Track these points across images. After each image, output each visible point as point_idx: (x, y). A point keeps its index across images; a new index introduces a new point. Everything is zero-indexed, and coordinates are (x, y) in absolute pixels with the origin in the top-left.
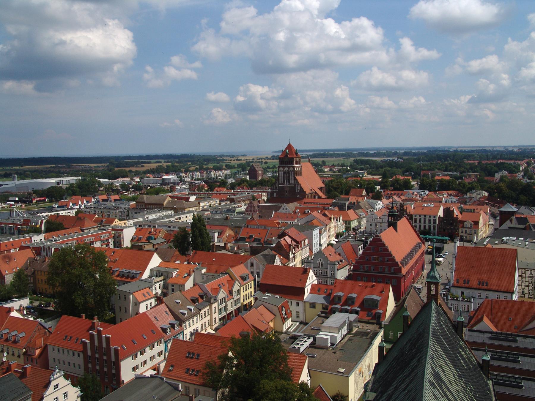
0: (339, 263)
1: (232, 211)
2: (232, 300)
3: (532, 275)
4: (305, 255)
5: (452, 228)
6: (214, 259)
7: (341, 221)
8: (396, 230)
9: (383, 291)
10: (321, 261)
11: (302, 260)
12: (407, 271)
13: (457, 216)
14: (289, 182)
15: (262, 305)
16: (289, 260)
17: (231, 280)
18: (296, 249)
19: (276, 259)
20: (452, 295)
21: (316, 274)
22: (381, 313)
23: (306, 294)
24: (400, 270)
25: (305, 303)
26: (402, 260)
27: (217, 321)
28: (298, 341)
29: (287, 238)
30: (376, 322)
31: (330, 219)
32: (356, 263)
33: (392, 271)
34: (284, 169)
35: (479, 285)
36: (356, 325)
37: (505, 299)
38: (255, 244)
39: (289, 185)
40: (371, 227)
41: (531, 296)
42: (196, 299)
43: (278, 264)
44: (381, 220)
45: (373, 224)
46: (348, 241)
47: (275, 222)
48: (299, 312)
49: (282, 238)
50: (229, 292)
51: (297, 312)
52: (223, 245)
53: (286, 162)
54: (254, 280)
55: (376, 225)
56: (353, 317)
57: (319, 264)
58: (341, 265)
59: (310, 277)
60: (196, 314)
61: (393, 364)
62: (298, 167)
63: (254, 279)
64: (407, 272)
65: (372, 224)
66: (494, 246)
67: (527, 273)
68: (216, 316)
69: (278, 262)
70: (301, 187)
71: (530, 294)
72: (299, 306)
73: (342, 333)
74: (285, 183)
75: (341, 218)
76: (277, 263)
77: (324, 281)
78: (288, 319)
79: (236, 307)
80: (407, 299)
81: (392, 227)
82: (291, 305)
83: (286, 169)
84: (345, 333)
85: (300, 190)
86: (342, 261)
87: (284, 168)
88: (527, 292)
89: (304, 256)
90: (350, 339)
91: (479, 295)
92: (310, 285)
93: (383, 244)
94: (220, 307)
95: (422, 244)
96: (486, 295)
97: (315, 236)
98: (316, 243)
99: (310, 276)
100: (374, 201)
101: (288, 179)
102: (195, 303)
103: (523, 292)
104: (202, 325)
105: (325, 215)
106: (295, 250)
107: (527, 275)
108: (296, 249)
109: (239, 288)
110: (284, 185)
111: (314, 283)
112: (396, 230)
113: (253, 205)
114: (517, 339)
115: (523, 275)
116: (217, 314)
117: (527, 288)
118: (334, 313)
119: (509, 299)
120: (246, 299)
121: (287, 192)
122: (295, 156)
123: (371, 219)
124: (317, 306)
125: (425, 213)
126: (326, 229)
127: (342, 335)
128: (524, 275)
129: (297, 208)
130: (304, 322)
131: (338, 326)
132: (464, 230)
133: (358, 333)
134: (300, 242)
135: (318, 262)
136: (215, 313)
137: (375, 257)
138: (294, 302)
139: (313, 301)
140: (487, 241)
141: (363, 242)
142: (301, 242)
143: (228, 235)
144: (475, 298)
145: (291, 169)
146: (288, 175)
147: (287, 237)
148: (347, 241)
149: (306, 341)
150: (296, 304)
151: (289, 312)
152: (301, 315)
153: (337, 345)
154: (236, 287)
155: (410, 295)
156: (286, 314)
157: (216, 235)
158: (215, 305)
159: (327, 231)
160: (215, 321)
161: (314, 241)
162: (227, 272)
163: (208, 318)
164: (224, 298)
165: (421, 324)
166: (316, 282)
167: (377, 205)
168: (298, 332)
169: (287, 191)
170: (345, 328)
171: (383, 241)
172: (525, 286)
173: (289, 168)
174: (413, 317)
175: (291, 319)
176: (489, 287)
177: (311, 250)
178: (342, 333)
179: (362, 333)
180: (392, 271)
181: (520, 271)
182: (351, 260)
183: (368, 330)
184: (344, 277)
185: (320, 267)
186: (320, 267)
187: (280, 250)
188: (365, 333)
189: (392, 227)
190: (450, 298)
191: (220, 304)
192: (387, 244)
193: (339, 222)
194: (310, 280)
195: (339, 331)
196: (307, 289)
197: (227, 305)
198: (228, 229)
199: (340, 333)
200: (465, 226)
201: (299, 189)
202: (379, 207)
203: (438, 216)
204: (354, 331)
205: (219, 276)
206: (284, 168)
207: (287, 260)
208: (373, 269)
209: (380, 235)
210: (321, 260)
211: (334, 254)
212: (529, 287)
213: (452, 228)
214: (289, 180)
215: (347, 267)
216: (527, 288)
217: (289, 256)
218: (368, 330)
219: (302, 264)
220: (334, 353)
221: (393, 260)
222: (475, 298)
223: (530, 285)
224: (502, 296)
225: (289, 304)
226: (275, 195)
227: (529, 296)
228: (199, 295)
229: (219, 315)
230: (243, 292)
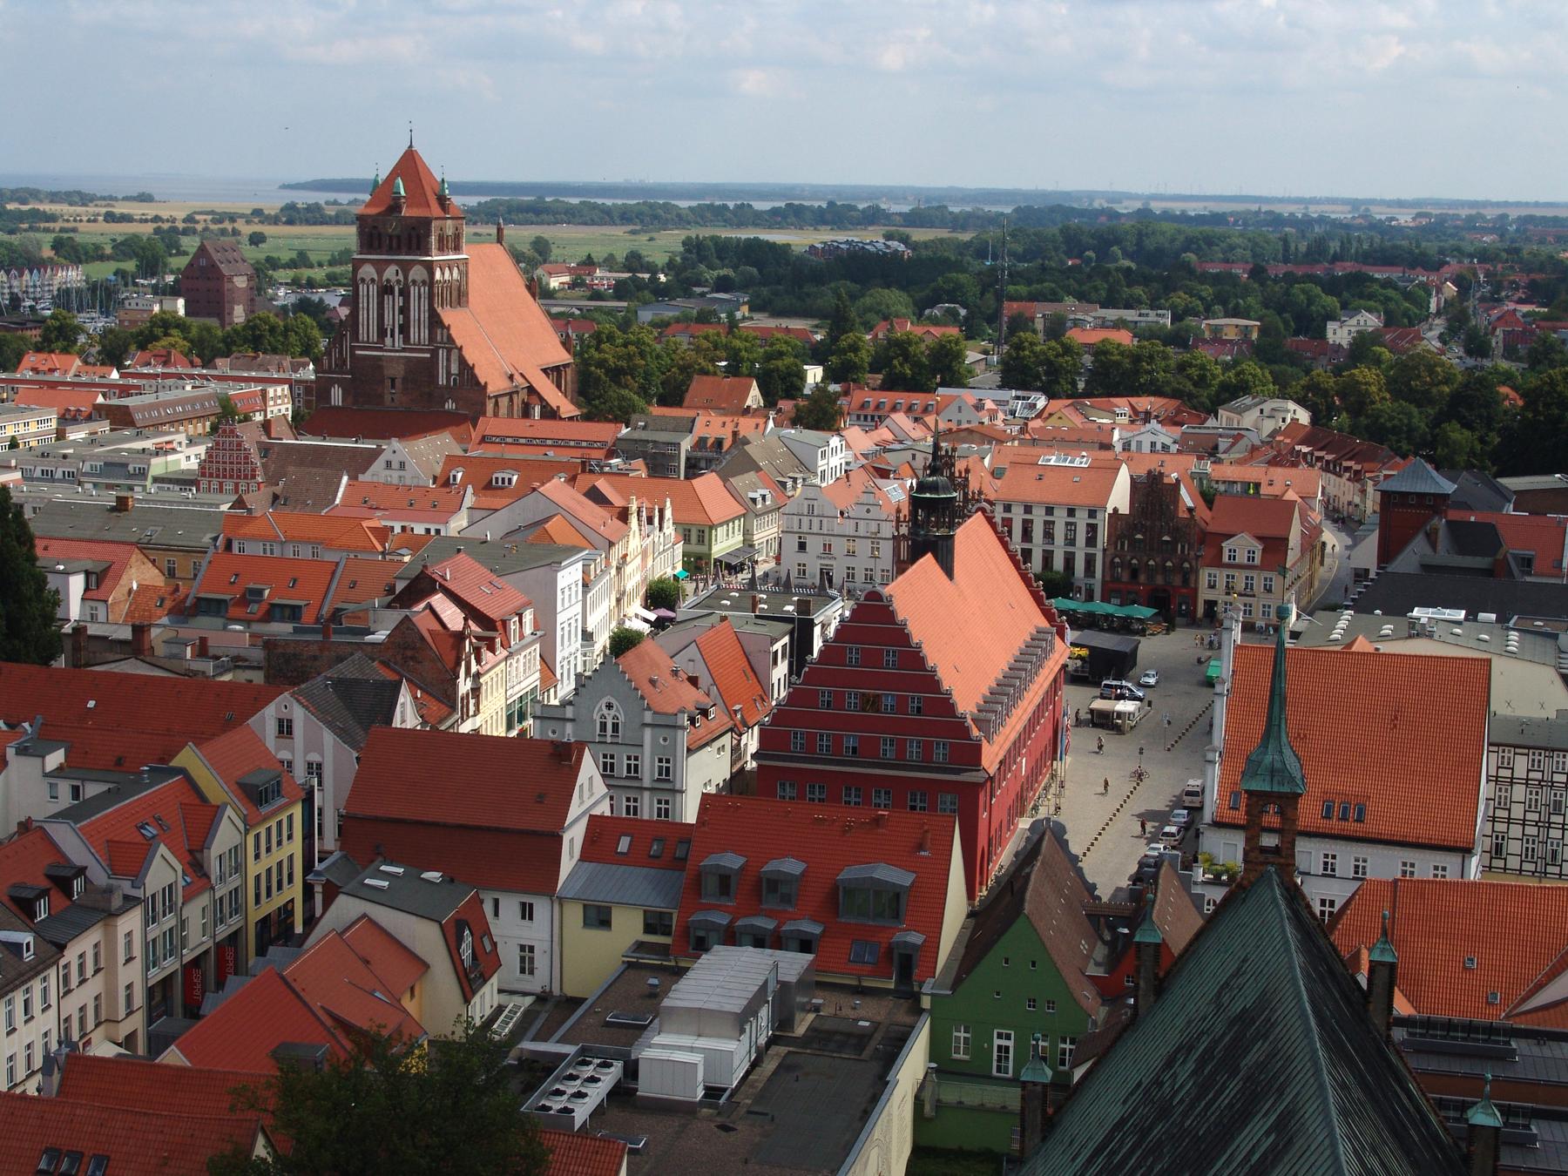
0: (692, 720)
1: (131, 468)
2: (204, 900)
3: (1539, 776)
4: (523, 685)
5: (1169, 564)
6: (91, 704)
7: (669, 528)
8: (949, 573)
9: (920, 847)
10: (613, 712)
11: (508, 707)
12: (1001, 757)
13: (1190, 510)
14: (407, 339)
15: (365, 916)
16: (453, 708)
17: (197, 801)
18: (487, 655)
19: (401, 700)
20: (1211, 861)
21: (608, 771)
22: (914, 946)
23: (568, 862)
24: (977, 749)
25: (561, 906)
26: (978, 705)
27: (139, 999)
28: (557, 1080)
29: (439, 601)
30: (892, 986)
31: (624, 515)
32: (775, 721)
33: (939, 755)
34: (380, 273)
35: (1328, 817)
36: (805, 1000)
37: (1435, 876)
38: (282, 629)
39: (404, 350)
40: (802, 558)
41: (1531, 867)
42: (38, 897)
43: (409, 725)
44: (853, 522)
45: (815, 545)
46: (724, 619)
47: (365, 524)
48: (532, 949)
49: (417, 601)
50: (189, 858)
51: (522, 948)
52: (126, 633)
53: (391, 237)
54: (304, 801)
55: (827, 548)
56: (793, 964)
57: (603, 726)
58: (702, 731)
59: (582, 786)
60: (38, 969)
61: (1113, 1153)
62: (450, 265)
63: (303, 795)
64: (1001, 762)
65: (809, 540)
66: (1385, 648)
67: (1521, 765)
68: (131, 975)
69: (406, 714)
70: (462, 362)
71: (1527, 855)
72: (531, 918)
73: (754, 1039)
74: (388, 340)
75: (668, 513)
76: (403, 721)
77: (625, 803)
78: (485, 981)
79: (223, 932)
80: (1033, 877)
81: (929, 555)
82: (496, 914)
83: (390, 273)
84: (762, 1040)
85: (460, 373)
86: (704, 713)
87: (380, 266)
88: (1514, 847)
89: (517, 689)
90: (784, 1067)
91: (1326, 863)
92: (584, 822)
93: (900, 635)
94: (155, 931)
95: (1057, 637)
96: (1357, 860)
97: (566, 590)
98: (567, 629)
99: (582, 778)
100: (811, 436)
101: (399, 319)
102: (32, 915)
103: (1499, 848)
104: (67, 1020)
105: (595, 496)
106: (479, 661)
107: (1520, 772)
109: (237, 839)
110: (380, 349)
111: (597, 811)
112: (949, 573)
113: (239, 444)
114: (1514, 1045)
115: (1503, 773)
116: (137, 964)
117: (1516, 831)
118: (702, 946)
119: (1452, 875)
120: (269, 894)
121: (393, 387)
122: (436, 210)
123: (805, 520)
124: (618, 916)
125: (1050, 499)
126: (608, 565)
127: (753, 1050)
128: (1507, 773)
129: (452, 461)
130: (556, 992)
131: (737, 1006)
132: (1221, 576)
133: (817, 1036)
134: (499, 624)
135: (596, 717)
136: (129, 960)
137: (863, 694)
138: (510, 905)
139: (600, 896)
140: (1342, 624)
141: (790, 626)
142: (504, 623)
143: (135, 587)
144: (1308, 874)
145: (417, 273)
146: (399, 301)
147: (440, 595)
148: (714, 619)
149: (593, 1080)
150: (517, 910)
151: (488, 948)
152: (541, 962)
153: (731, 1095)
154: (226, 836)
155: (1042, 863)
156: (474, 956)
157: (77, 584)
158: (131, 922)
159: (613, 572)
160: (129, 998)
161: (560, 618)
162: (174, 763)
163: (95, 986)
164: (170, 886)
165: (1237, 973)
166: (604, 809)
167: (824, 454)
168: (542, 1037)
169: (393, 380)
170: (764, 1013)
171: (900, 617)
172: (1509, 821)
173: (405, 267)
174: (1176, 951)
175: (494, 981)
176: (1370, 827)
177: (548, 663)
178: (754, 1039)
179: (838, 1037)
180: (939, 755)
181: (1493, 756)
182: (737, 707)
183: (861, 1023)
184: (714, 784)
185: (609, 740)
186: (609, 740)
187: (412, 658)
188: (849, 1035)
189: (929, 555)
190: (1201, 879)
191: (150, 919)
192: (917, 633)
193: (661, 529)
194: (581, 797)
195: (742, 1031)
196: (572, 840)
197: (183, 924)
198: (136, 556)
199: (745, 1038)
200: (1225, 559)
201: (454, 369)
202: (832, 464)
203: (1110, 510)
204: (800, 1030)
205: (139, 786)
206: (380, 266)
207: (445, 710)
208: (854, 749)
209: (886, 591)
210: (609, 706)
211: (672, 680)
212: (1524, 825)
213: (1169, 564)
214: (404, 329)
215: (726, 740)
216: (1516, 831)
217: (455, 687)
218: (861, 1023)
219: (510, 727)
220: (725, 1128)
221: (945, 705)
222: (1308, 874)
223: (1529, 816)
224: (1425, 866)
225: (488, 908)
226: (337, 396)
227: (1526, 866)
228: (49, 877)
229: (148, 969)
230: (257, 856)
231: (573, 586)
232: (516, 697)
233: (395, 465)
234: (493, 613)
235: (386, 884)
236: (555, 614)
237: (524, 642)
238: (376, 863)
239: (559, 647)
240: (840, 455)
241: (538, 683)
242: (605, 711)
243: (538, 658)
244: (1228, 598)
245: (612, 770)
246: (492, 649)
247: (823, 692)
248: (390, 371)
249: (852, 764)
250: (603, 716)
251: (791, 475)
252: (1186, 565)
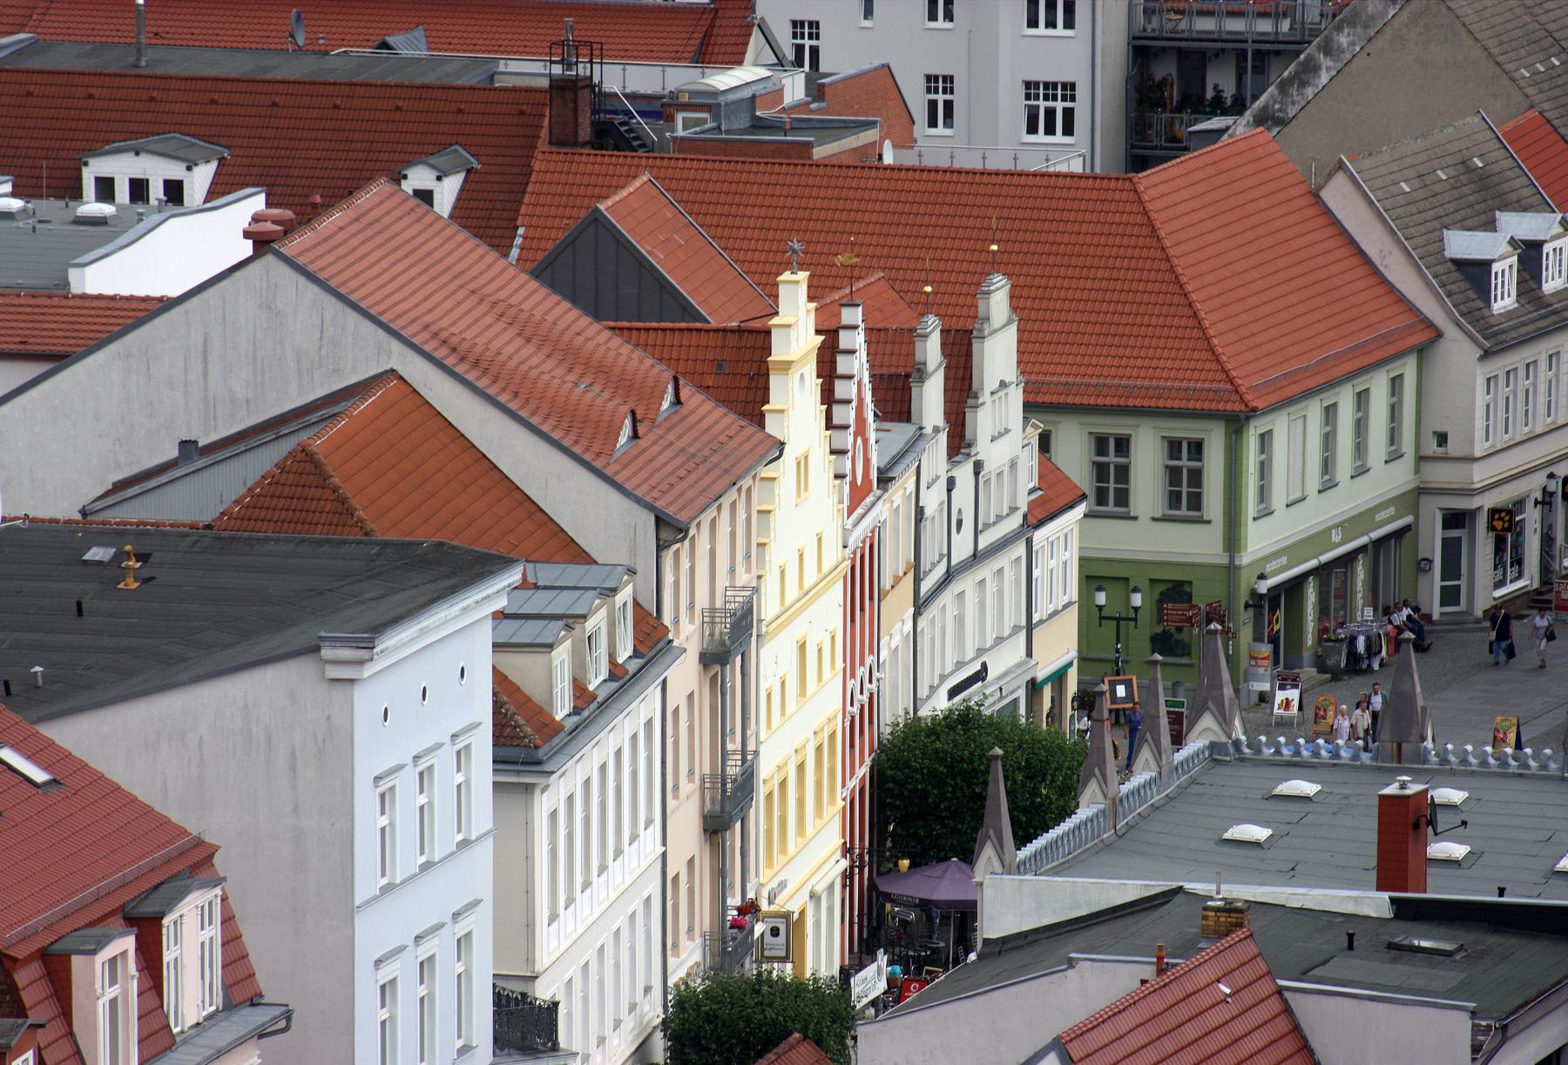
159: (684, 674)
193: (959, 443)
231: (443, 761)
236: (345, 911)
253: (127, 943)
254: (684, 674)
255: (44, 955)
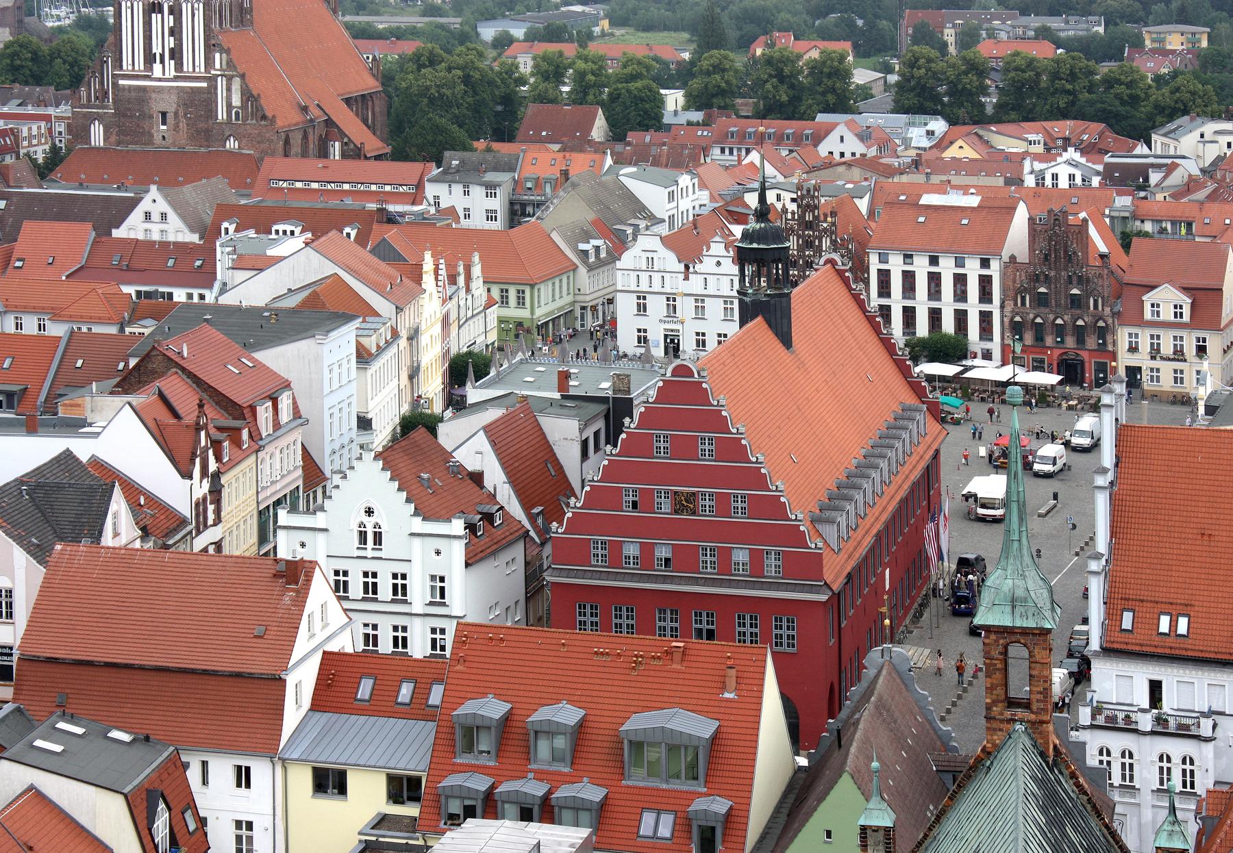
4: (278, 486)
7: (478, 287)
12: (848, 569)
14: (179, 67)
19: (113, 507)
23: (294, 712)
39: (176, 78)
40: (642, 323)
43: (122, 540)
45: (656, 306)
57: (363, 536)
64: (849, 576)
65: (650, 300)
74: (157, 68)
75: (477, 271)
76: (116, 534)
80: (861, 726)
85: (244, 106)
89: (269, 492)
92: (316, 659)
97: (336, 370)
98: (337, 415)
101: (170, 42)
106: (218, 458)
108: (226, 444)
111: (333, 647)
123: (644, 277)
124: (354, 780)
126: (395, 334)
134: (247, 412)
137: (676, 493)
141: (601, 408)
142: (253, 409)
146: (170, 21)
155: (877, 707)
159: (403, 342)
166: (347, 643)
180: (771, 565)
193: (468, 290)
200: (1148, 315)
201: (236, 101)
210: (369, 512)
214: (176, 54)
226: (97, 134)
231: (345, 362)
232: (270, 502)
233: (156, 217)
234: (242, 399)
235: (58, 748)
237: (279, 433)
238: (54, 718)
239: (327, 438)
240: (691, 197)
241: (300, 483)
242: (365, 519)
243: (300, 452)
244: (1155, 364)
245: (375, 592)
246: (237, 443)
247: (627, 490)
248: (157, 106)
249: (665, 579)
250: (362, 525)
251: (632, 221)
252: (1101, 324)
253: (270, 404)
254: (403, 342)
255: (250, 406)
